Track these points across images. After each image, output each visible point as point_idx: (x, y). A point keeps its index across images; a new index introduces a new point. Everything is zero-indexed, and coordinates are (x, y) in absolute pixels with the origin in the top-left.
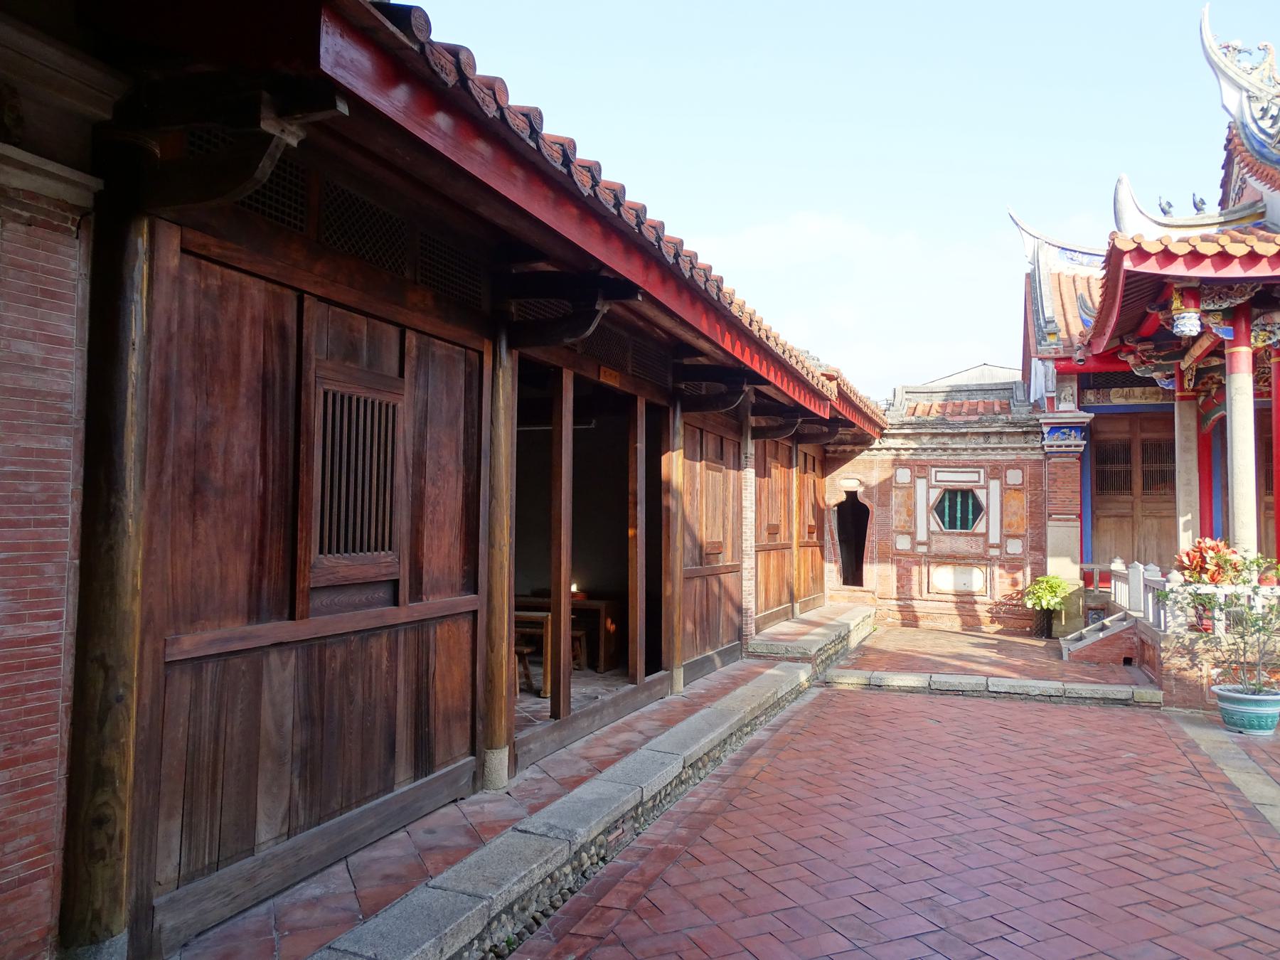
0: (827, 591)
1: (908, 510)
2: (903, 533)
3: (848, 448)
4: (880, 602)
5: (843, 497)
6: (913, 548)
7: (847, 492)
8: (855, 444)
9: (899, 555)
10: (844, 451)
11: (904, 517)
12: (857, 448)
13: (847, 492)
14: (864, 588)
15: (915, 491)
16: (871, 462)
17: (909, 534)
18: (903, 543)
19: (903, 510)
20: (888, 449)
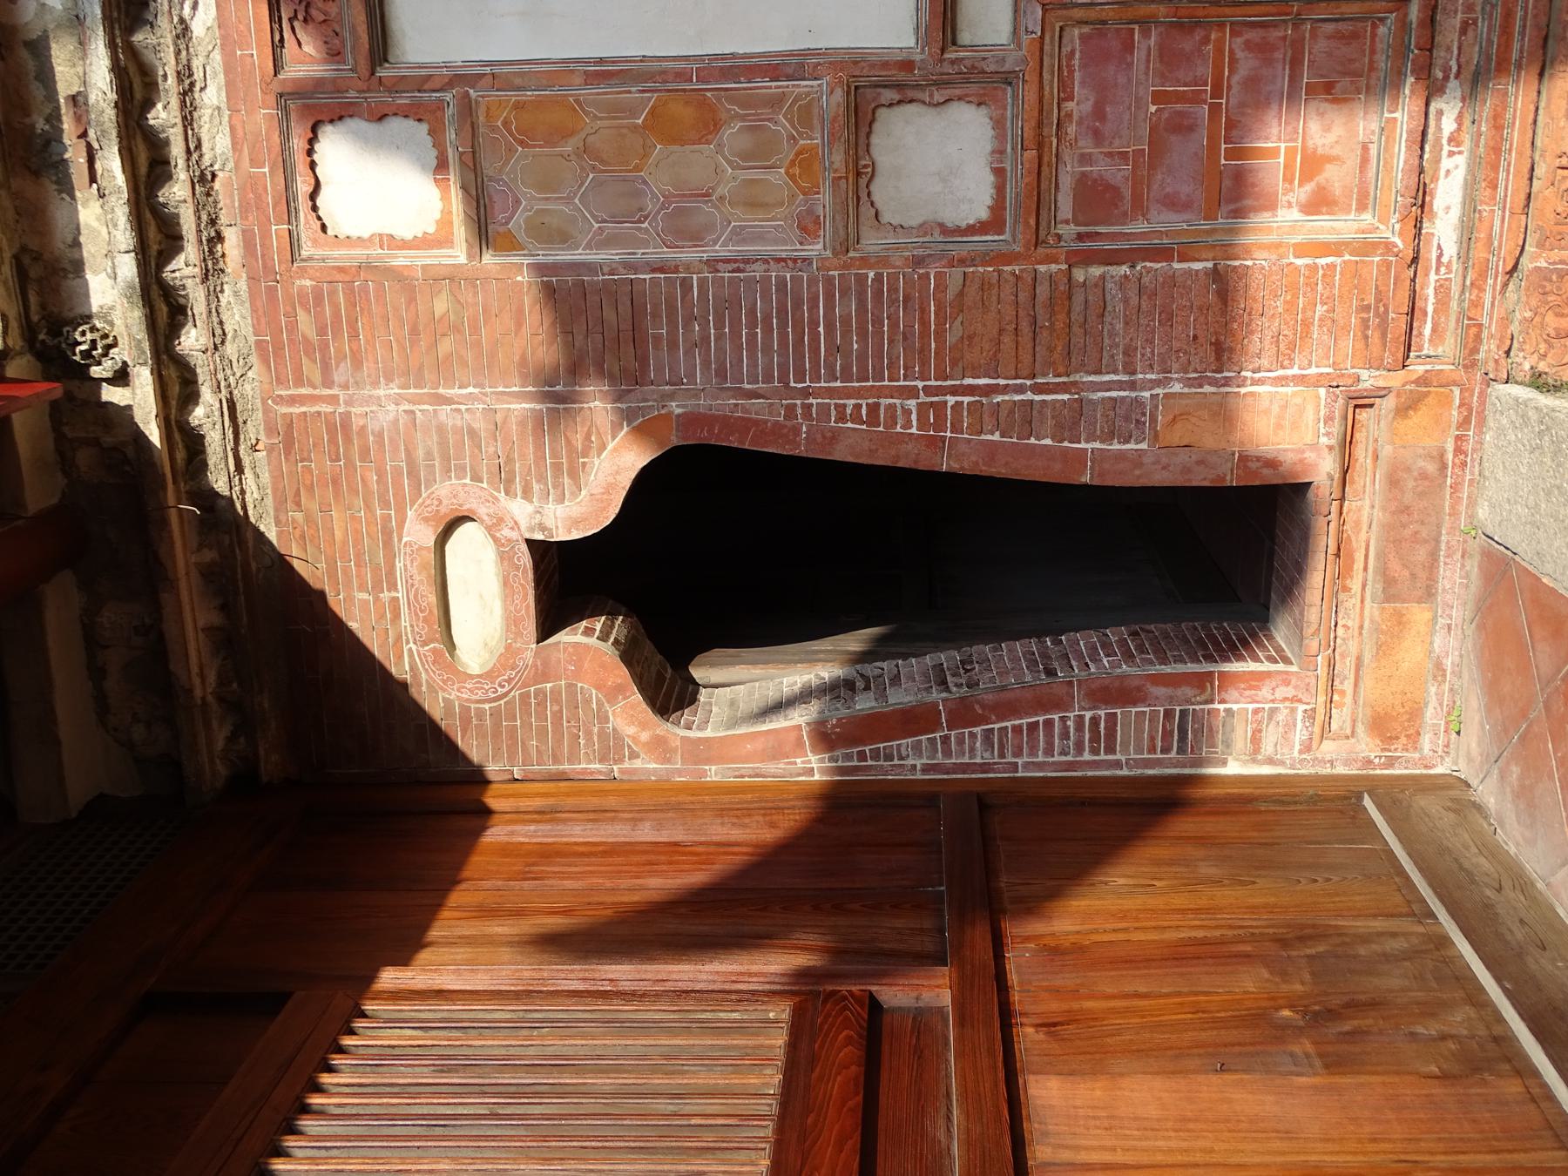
0: (1343, 754)
1: (660, 127)
2: (860, 172)
3: (193, 616)
4: (1438, 349)
5: (590, 644)
6: (979, 81)
7: (551, 619)
8: (151, 578)
9: (1039, 202)
10: (225, 641)
11: (715, 164)
12: (184, 556)
13: (551, 619)
14: (1323, 470)
15: (495, 76)
16: (288, 438)
17: (859, 119)
18: (943, 165)
19: (667, 169)
20: (164, 310)
